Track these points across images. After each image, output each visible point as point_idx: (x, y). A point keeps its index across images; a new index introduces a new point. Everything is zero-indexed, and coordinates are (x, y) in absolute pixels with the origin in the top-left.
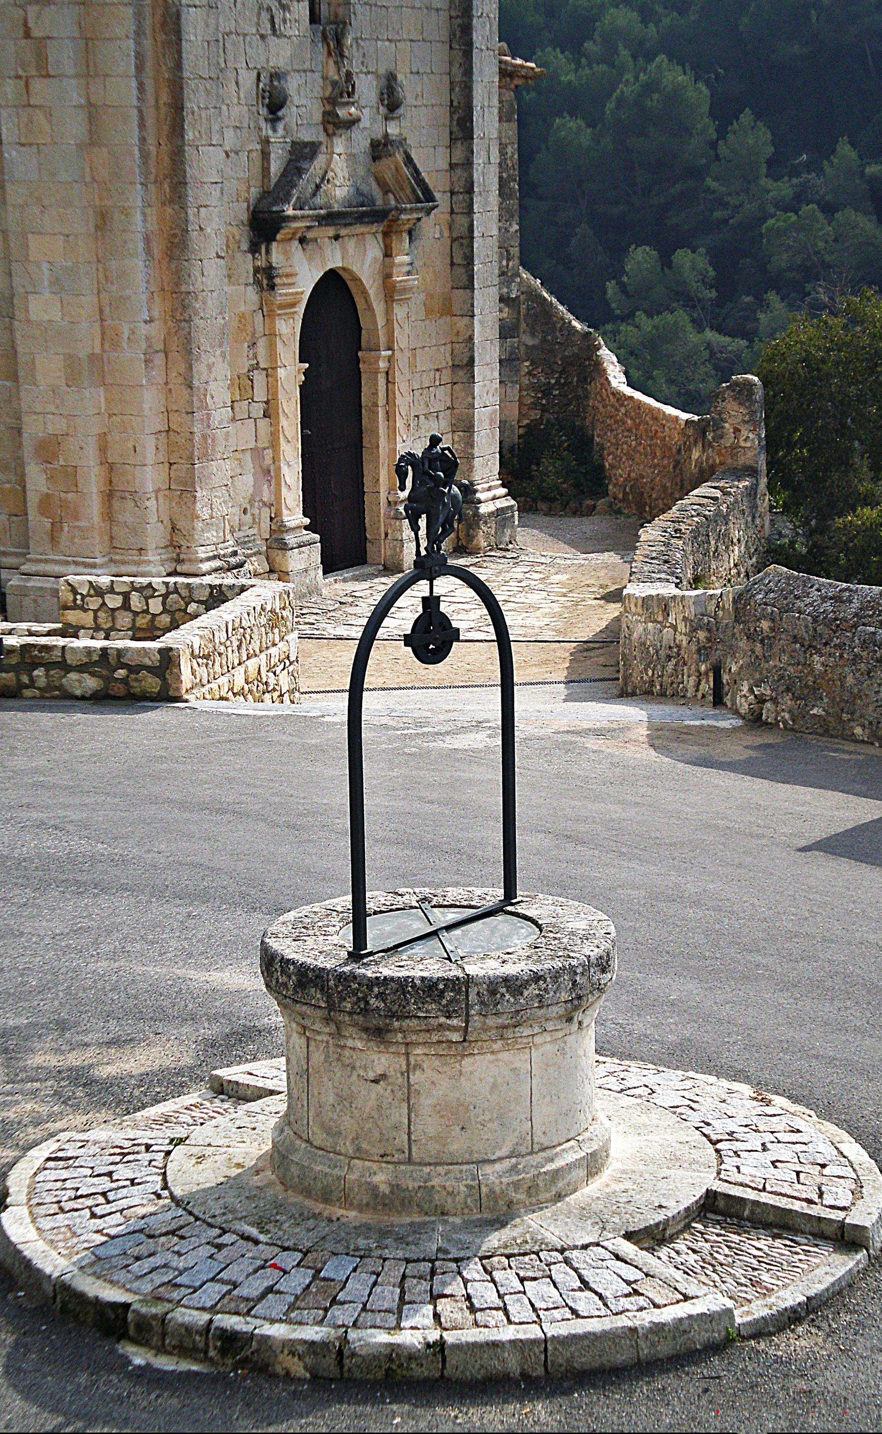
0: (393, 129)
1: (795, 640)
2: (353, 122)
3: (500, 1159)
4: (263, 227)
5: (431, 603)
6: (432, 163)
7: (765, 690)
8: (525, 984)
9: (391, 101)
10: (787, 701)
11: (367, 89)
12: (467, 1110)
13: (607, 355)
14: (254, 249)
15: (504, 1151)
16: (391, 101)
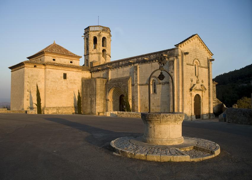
0: (203, 84)
1: (232, 114)
2: (199, 83)
3: (165, 139)
4: (191, 90)
5: (161, 73)
6: (207, 87)
7: (229, 119)
8: (168, 116)
9: (202, 82)
10: (231, 120)
11: (200, 81)
12: (161, 132)
13: (224, 105)
14: (190, 92)
15: (166, 138)
16: (202, 82)
